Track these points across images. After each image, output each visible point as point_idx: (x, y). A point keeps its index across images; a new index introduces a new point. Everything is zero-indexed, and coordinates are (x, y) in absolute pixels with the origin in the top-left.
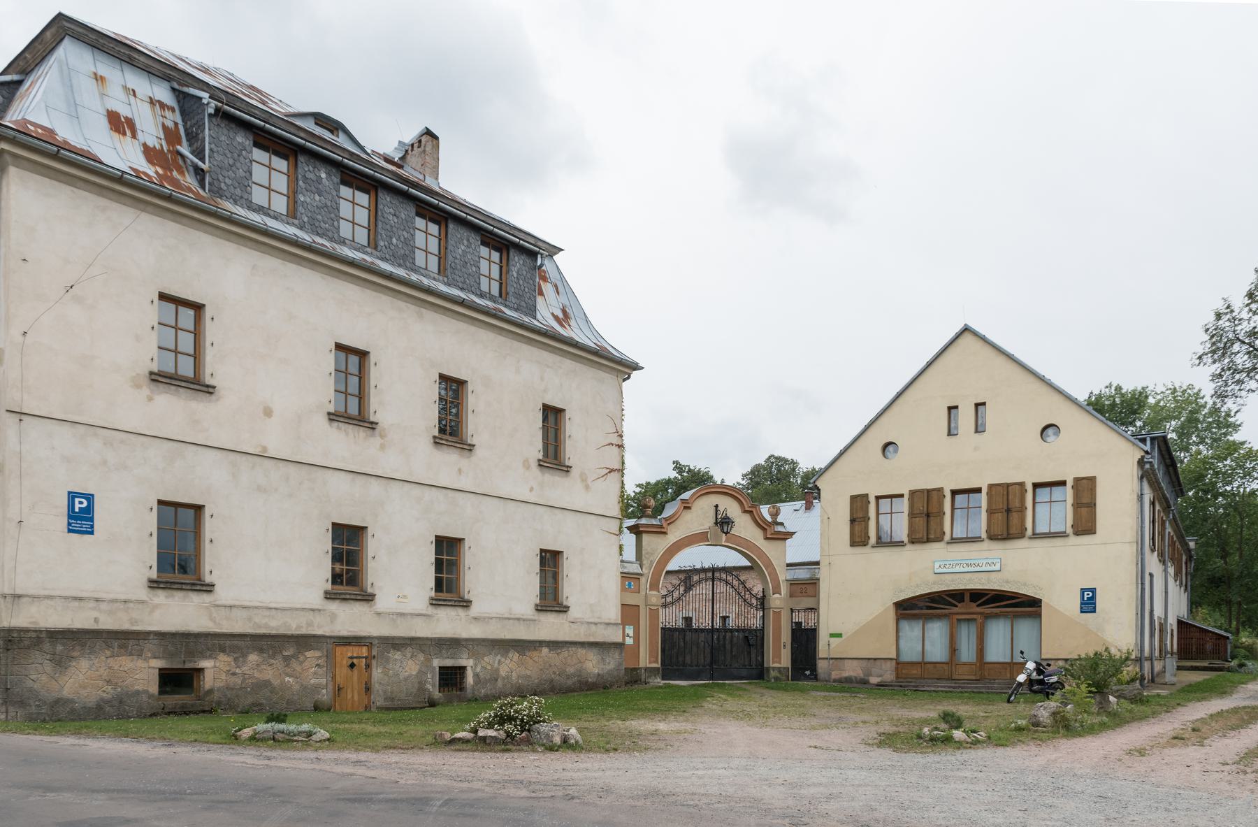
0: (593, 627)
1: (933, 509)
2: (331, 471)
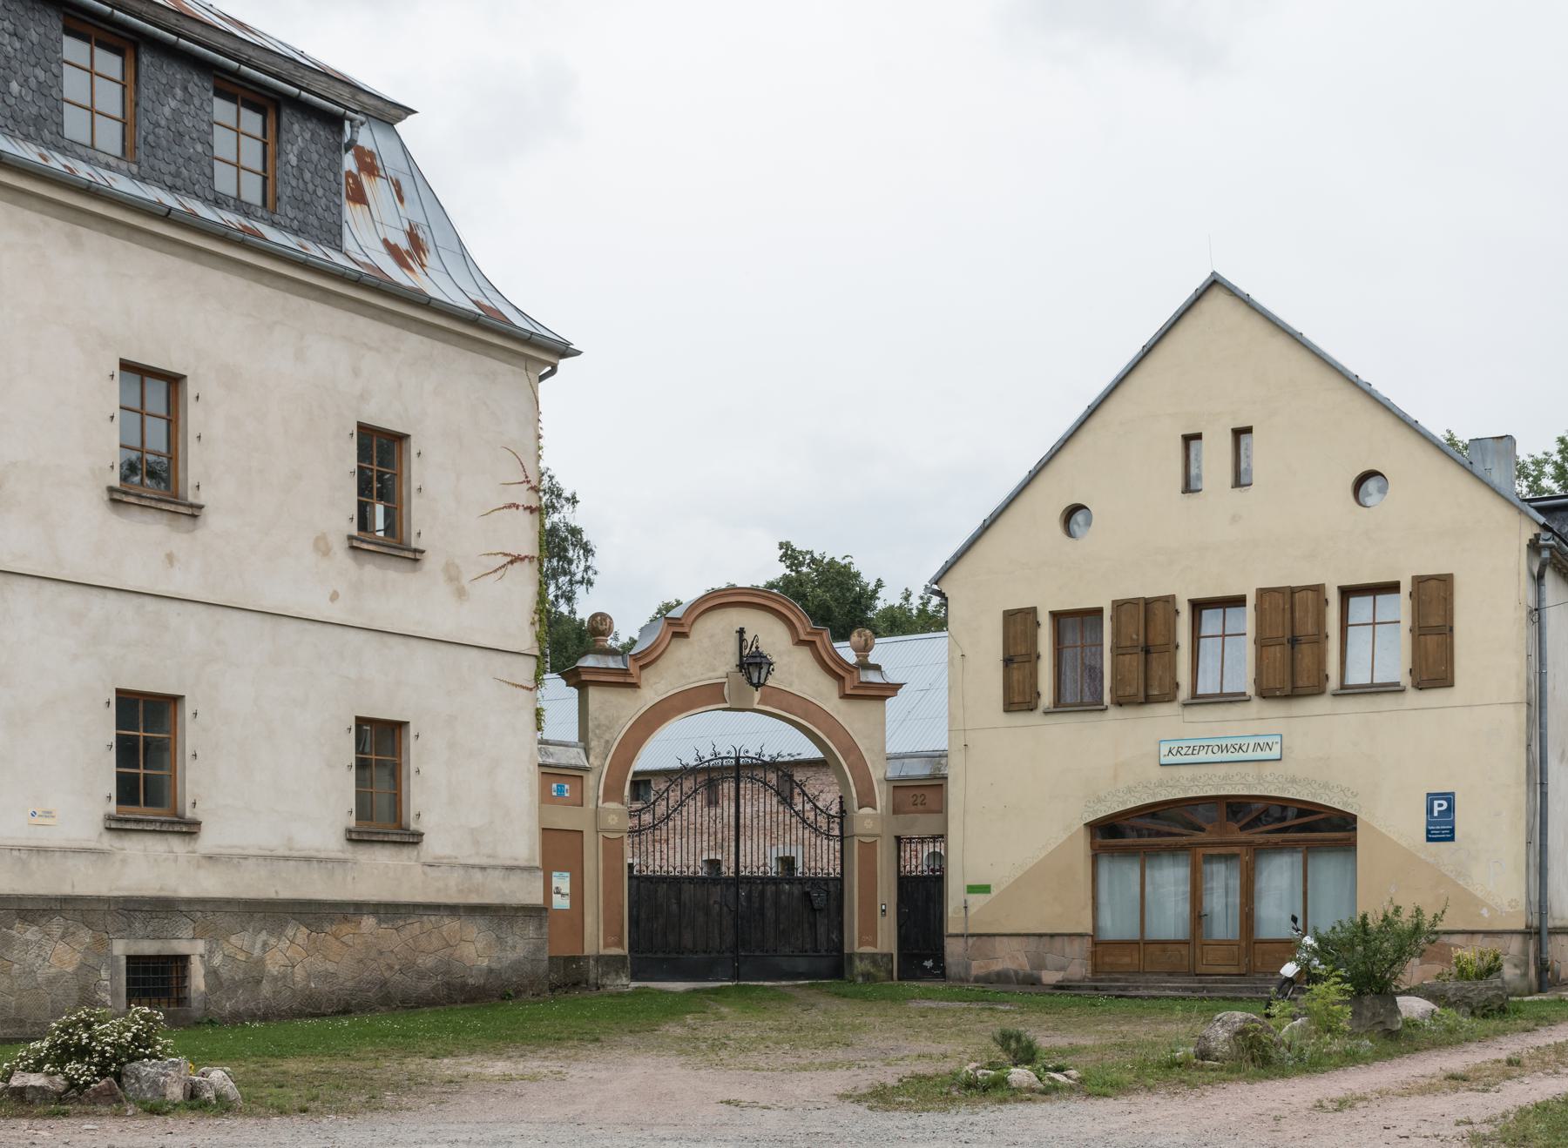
0: (478, 876)
1: (1158, 639)
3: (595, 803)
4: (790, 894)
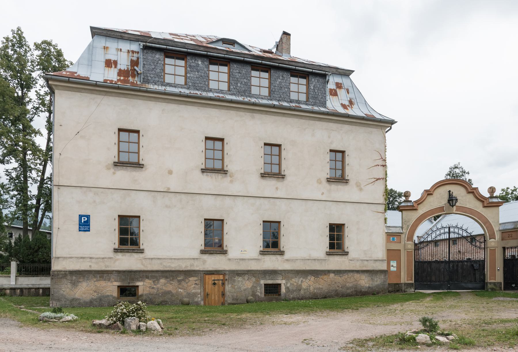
0: (366, 263)
2: (204, 195)
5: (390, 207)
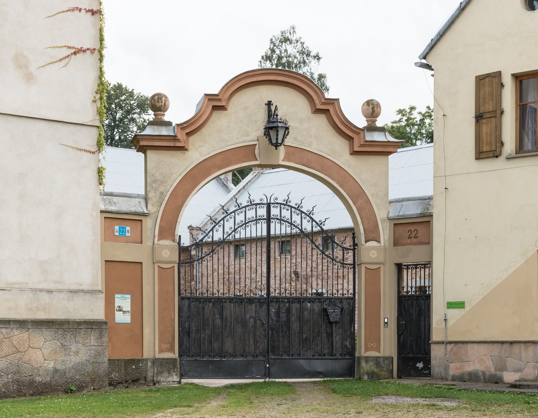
0: (45, 297)
3: (152, 241)
4: (312, 310)
5: (117, 138)
